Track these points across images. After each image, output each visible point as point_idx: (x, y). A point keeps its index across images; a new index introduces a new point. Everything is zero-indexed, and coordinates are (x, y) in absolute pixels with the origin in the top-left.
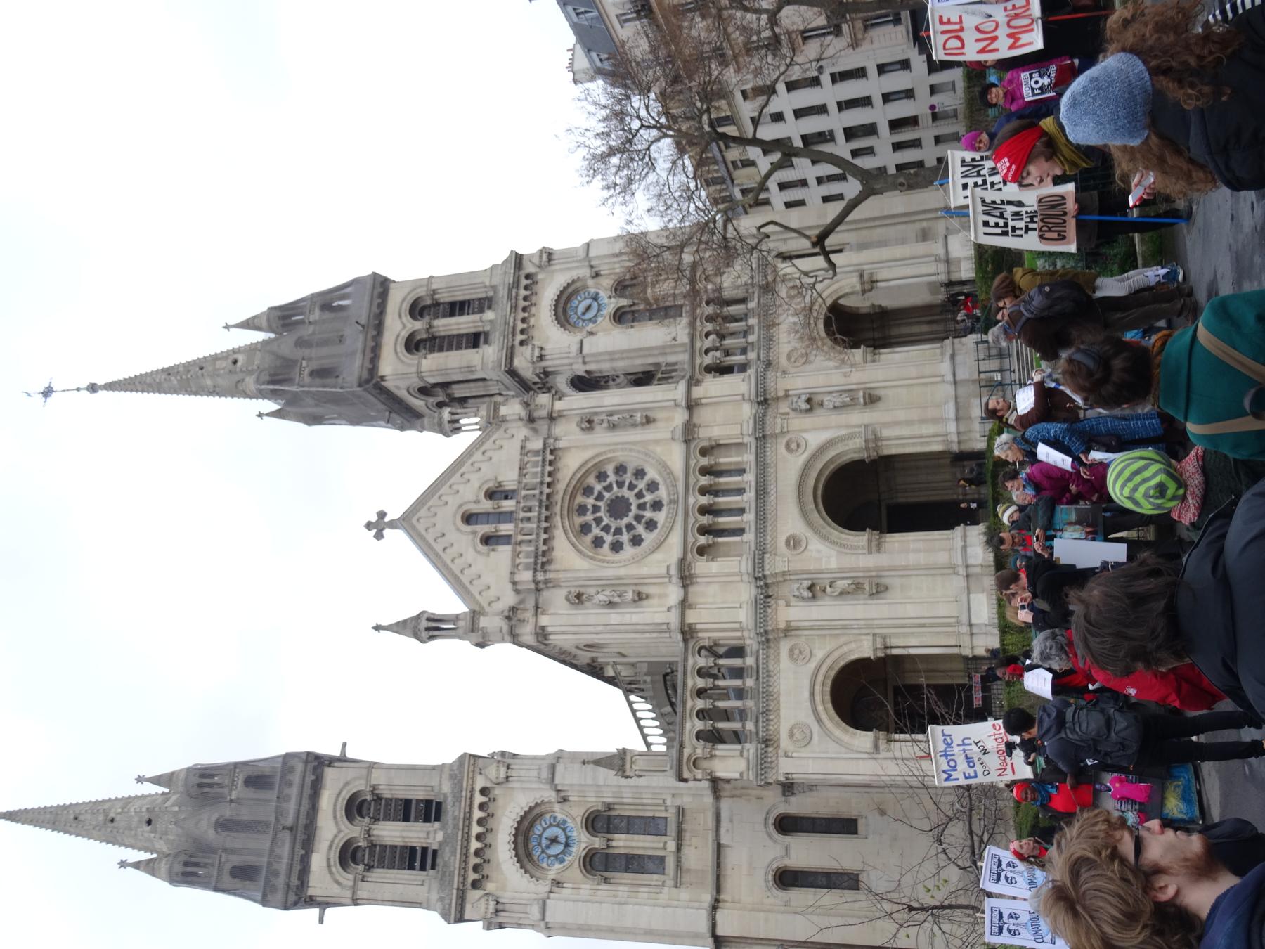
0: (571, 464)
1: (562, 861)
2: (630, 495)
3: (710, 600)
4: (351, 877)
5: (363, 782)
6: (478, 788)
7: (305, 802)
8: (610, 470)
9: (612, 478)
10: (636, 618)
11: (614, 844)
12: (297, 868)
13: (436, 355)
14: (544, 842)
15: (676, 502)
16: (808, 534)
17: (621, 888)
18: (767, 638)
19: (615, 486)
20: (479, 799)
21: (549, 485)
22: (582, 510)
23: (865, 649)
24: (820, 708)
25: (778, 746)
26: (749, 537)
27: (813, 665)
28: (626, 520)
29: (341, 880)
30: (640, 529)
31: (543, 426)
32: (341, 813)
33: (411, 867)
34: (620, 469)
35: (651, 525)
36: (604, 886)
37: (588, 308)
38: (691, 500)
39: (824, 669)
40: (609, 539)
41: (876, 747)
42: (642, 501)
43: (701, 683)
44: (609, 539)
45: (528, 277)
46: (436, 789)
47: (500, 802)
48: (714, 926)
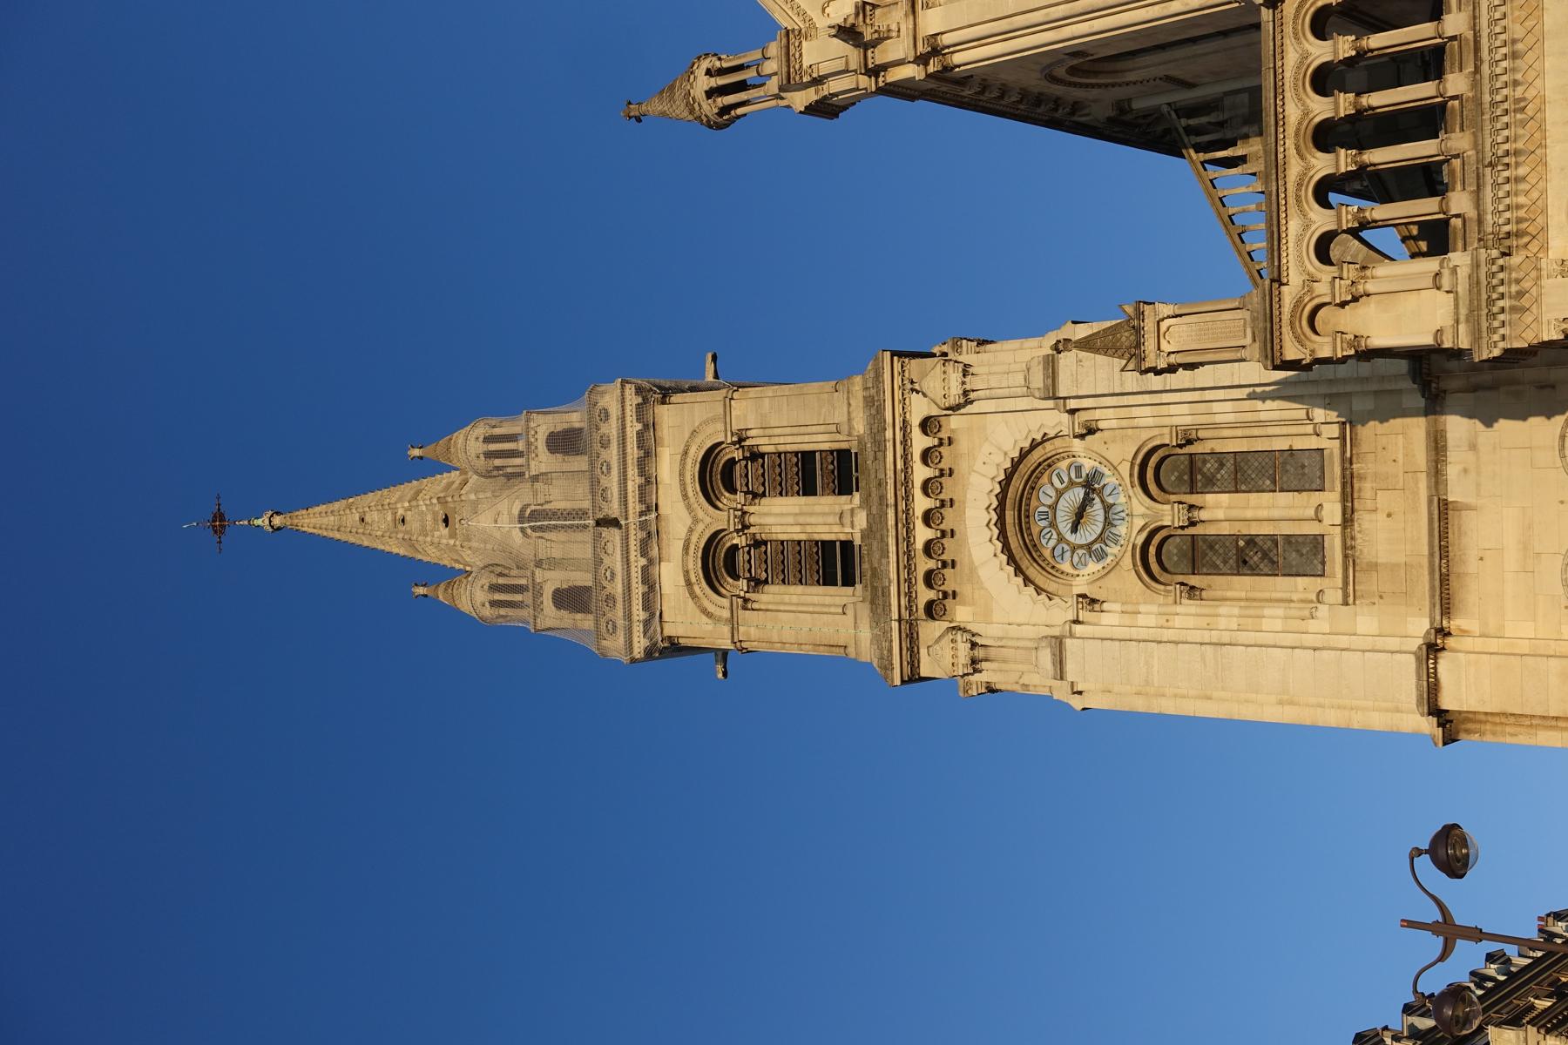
1: (1101, 556)
4: (725, 602)
5: (720, 426)
6: (915, 421)
7: (632, 471)
11: (1203, 515)
12: (638, 589)
17: (1223, 610)
20: (920, 442)
25: (1544, 247)
29: (711, 608)
32: (693, 488)
33: (829, 580)
36: (1189, 607)
46: (845, 429)
47: (963, 444)
48: (1431, 692)
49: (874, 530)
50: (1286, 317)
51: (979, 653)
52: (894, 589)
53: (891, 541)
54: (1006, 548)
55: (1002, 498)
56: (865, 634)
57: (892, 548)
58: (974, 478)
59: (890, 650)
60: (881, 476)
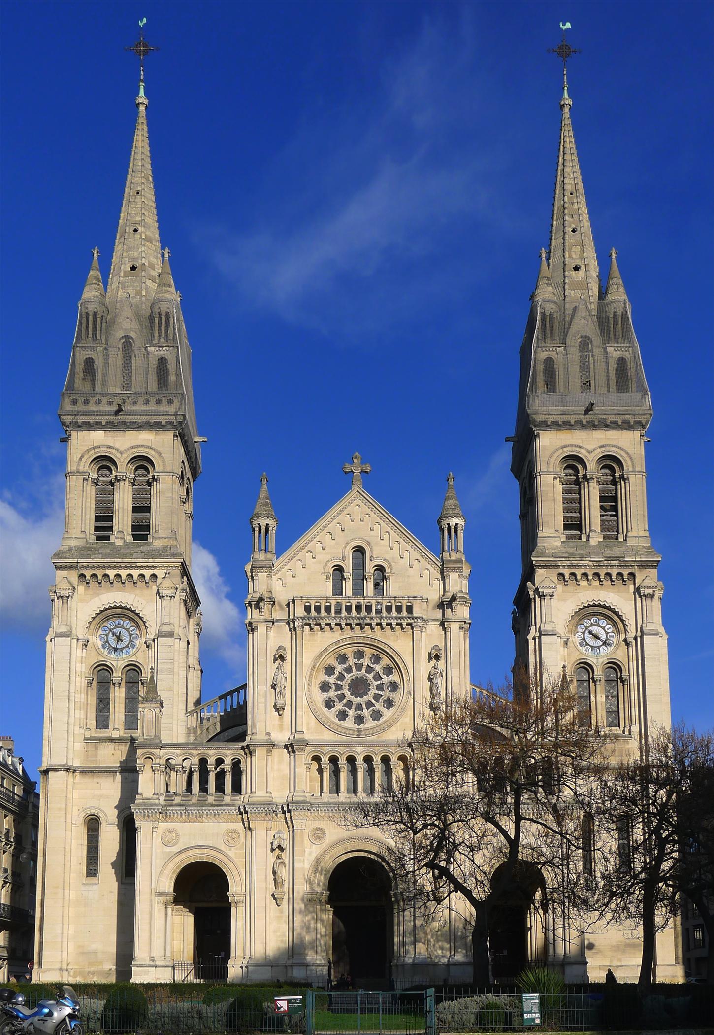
0: (398, 643)
2: (370, 697)
3: (276, 767)
6: (156, 572)
8: (395, 677)
9: (386, 679)
10: (261, 706)
13: (559, 488)
14: (117, 631)
15: (358, 736)
16: (324, 845)
18: (243, 812)
19: (379, 682)
20: (148, 573)
21: (380, 624)
22: (360, 655)
23: (235, 889)
24: (190, 853)
26: (327, 797)
27: (222, 848)
28: (347, 693)
29: (84, 460)
30: (339, 706)
31: (438, 614)
33: (98, 519)
34: (394, 686)
35: (343, 715)
37: (596, 637)
38: (359, 749)
39: (220, 856)
40: (332, 680)
41: (161, 894)
42: (364, 706)
43: (211, 761)
44: (332, 680)
45: (632, 575)
47: (146, 592)
49: (116, 552)
50: (150, 750)
51: (65, 599)
52: (89, 561)
53: (109, 560)
54: (106, 609)
55: (125, 608)
56: (73, 543)
57: (106, 561)
58: (133, 596)
59: (65, 558)
60: (135, 555)
